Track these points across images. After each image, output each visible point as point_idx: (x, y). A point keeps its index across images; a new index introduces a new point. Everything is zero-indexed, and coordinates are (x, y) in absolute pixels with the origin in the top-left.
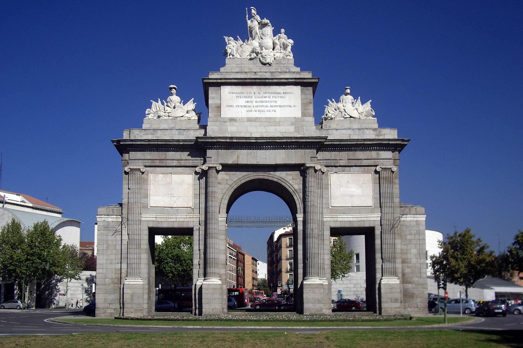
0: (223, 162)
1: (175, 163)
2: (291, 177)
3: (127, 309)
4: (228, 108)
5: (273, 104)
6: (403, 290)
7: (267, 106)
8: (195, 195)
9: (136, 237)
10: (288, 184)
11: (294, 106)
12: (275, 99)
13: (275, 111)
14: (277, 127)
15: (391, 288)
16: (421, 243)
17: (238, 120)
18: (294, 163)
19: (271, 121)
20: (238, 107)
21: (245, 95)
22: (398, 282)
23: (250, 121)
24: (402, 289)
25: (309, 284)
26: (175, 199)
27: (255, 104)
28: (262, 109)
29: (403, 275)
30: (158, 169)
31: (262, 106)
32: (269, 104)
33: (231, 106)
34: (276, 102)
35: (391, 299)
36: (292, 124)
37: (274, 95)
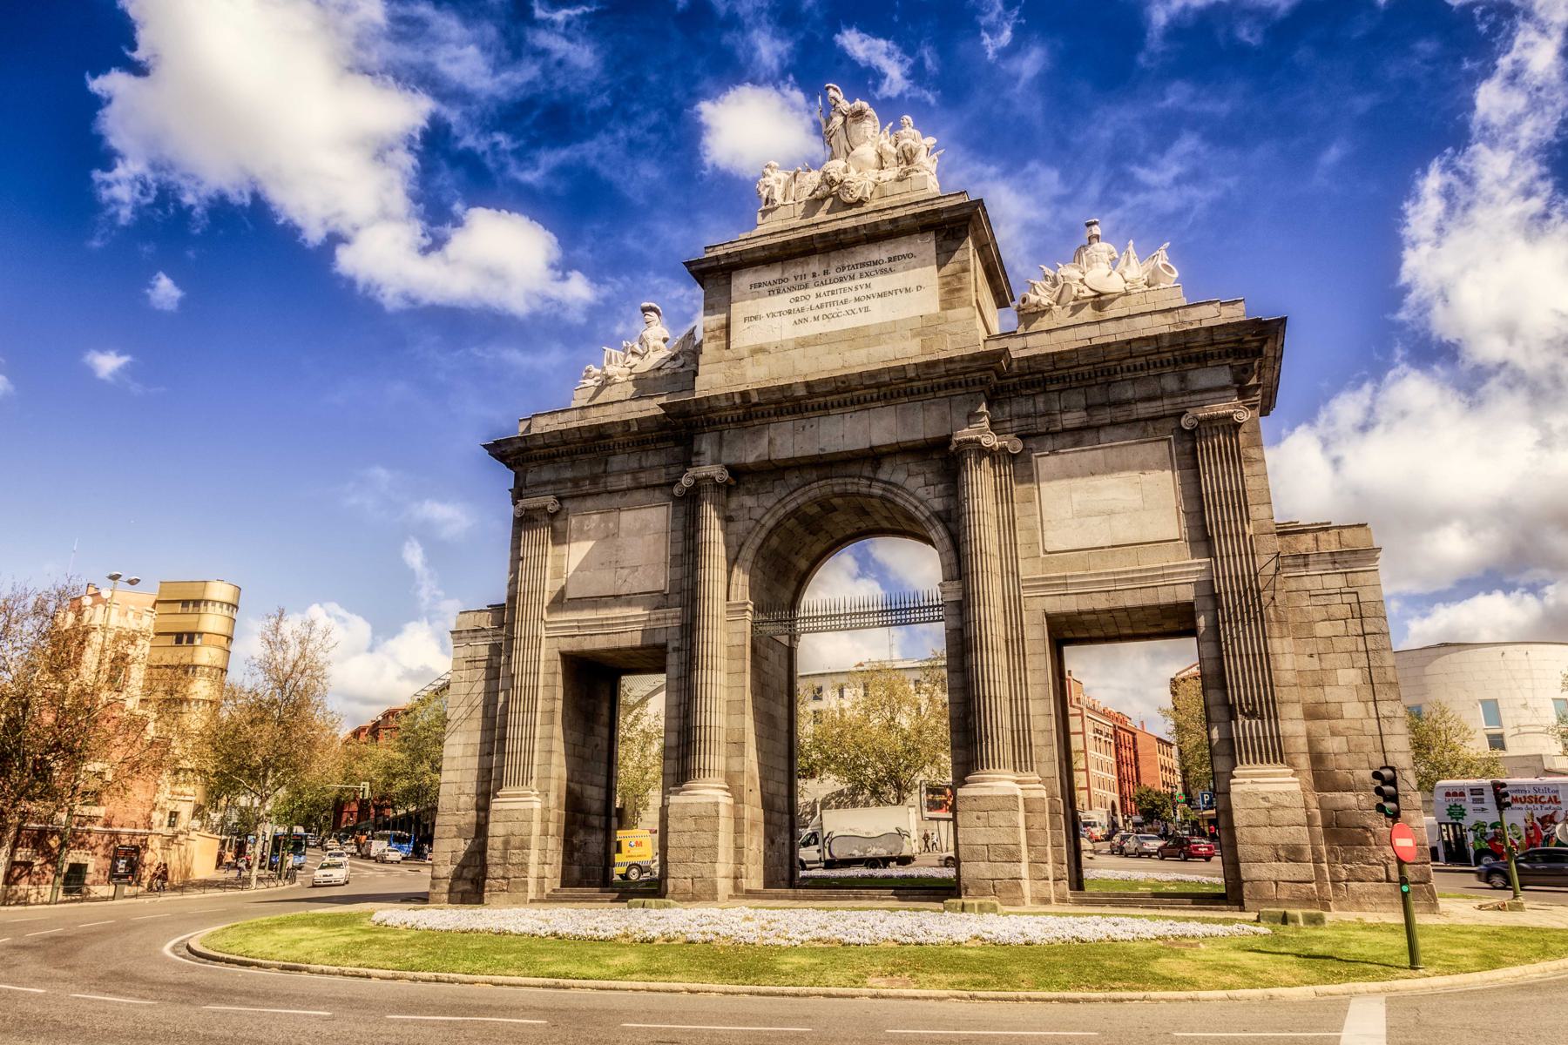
0: (732, 460)
1: (627, 481)
2: (921, 480)
3: (493, 882)
4: (748, 324)
5: (862, 292)
6: (1322, 813)
7: (845, 302)
8: (674, 557)
9: (529, 681)
10: (911, 499)
11: (919, 288)
12: (866, 280)
13: (867, 309)
14: (871, 350)
15: (1268, 810)
16: (1371, 646)
17: (772, 349)
18: (921, 436)
19: (855, 337)
20: (774, 315)
21: (792, 282)
22: (1296, 787)
23: (803, 346)
24: (1318, 812)
25: (975, 798)
26: (626, 572)
27: (814, 302)
28: (833, 310)
29: (1317, 758)
30: (589, 503)
31: (832, 304)
32: (851, 295)
33: (755, 318)
34: (868, 286)
35: (1275, 846)
36: (917, 333)
37: (866, 269)
